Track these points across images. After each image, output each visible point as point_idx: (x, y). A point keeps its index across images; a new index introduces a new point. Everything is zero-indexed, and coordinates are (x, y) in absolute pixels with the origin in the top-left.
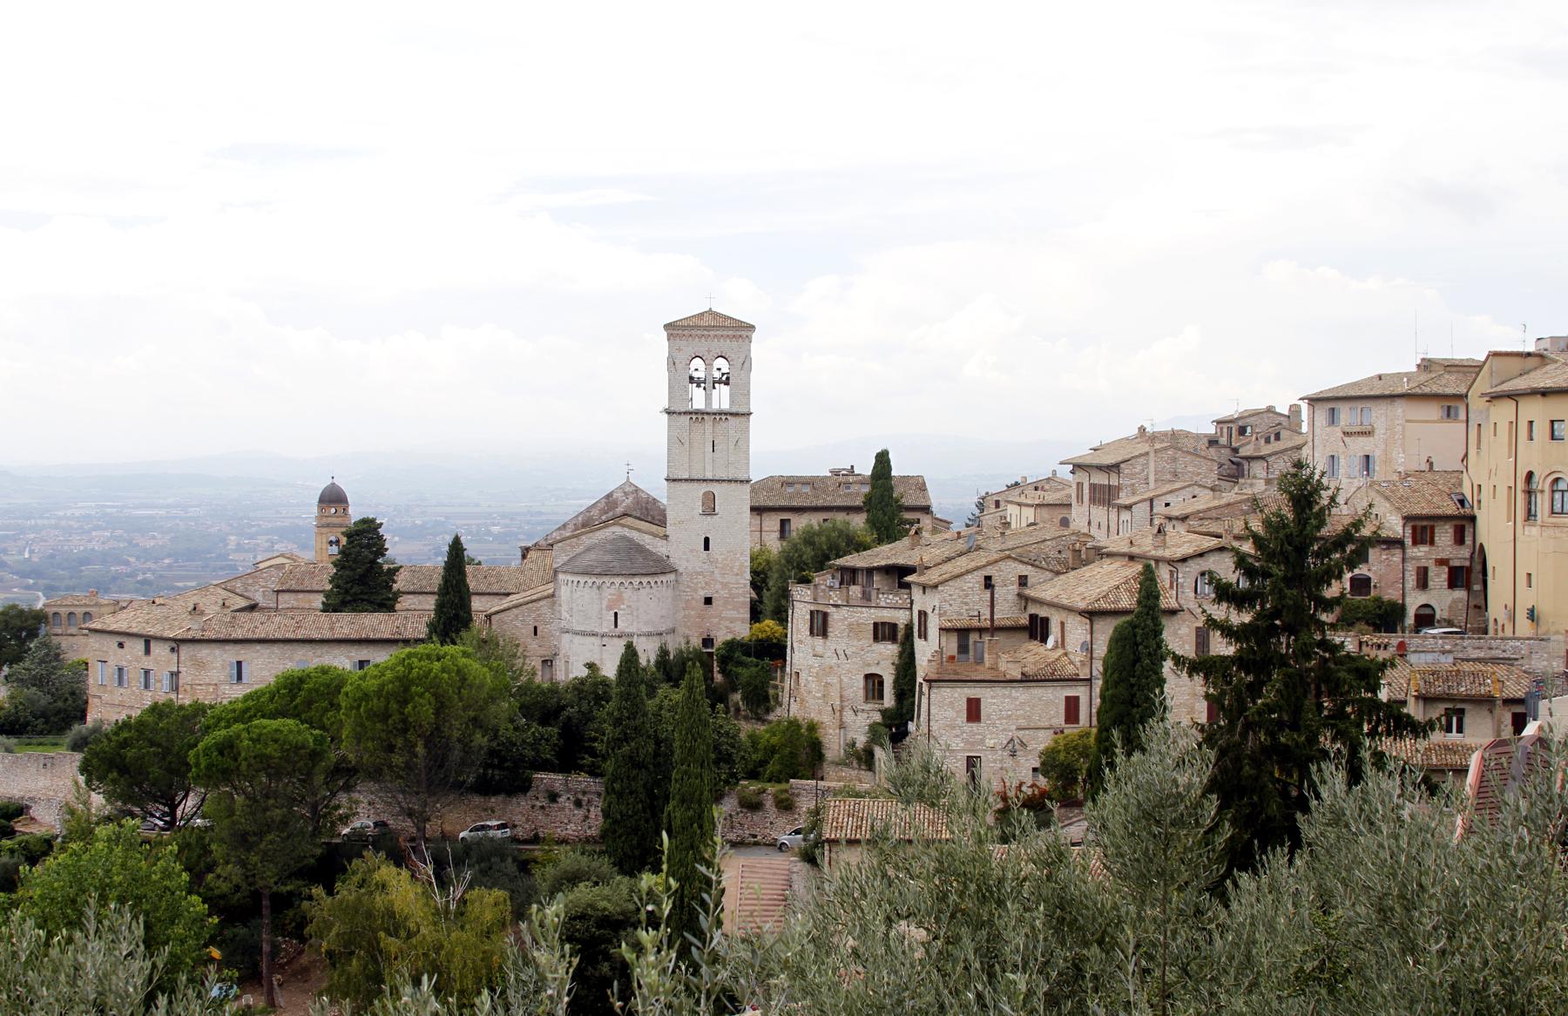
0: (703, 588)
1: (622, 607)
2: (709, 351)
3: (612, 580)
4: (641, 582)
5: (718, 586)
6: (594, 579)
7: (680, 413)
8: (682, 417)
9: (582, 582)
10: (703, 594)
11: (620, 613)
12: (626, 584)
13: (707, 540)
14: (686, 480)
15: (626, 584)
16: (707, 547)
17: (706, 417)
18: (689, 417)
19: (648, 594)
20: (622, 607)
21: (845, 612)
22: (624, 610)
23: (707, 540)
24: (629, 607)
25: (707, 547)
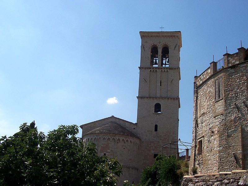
0: (154, 150)
1: (108, 151)
2: (160, 42)
3: (104, 137)
4: (119, 139)
5: (161, 149)
6: (96, 137)
7: (146, 68)
8: (147, 70)
9: (90, 138)
10: (153, 152)
11: (107, 154)
12: (111, 139)
13: (156, 126)
14: (147, 98)
15: (111, 139)
16: (156, 130)
17: (157, 70)
18: (149, 70)
19: (123, 146)
20: (108, 151)
21: (242, 69)
22: (109, 152)
23: (156, 126)
24: (111, 151)
25: (156, 130)
